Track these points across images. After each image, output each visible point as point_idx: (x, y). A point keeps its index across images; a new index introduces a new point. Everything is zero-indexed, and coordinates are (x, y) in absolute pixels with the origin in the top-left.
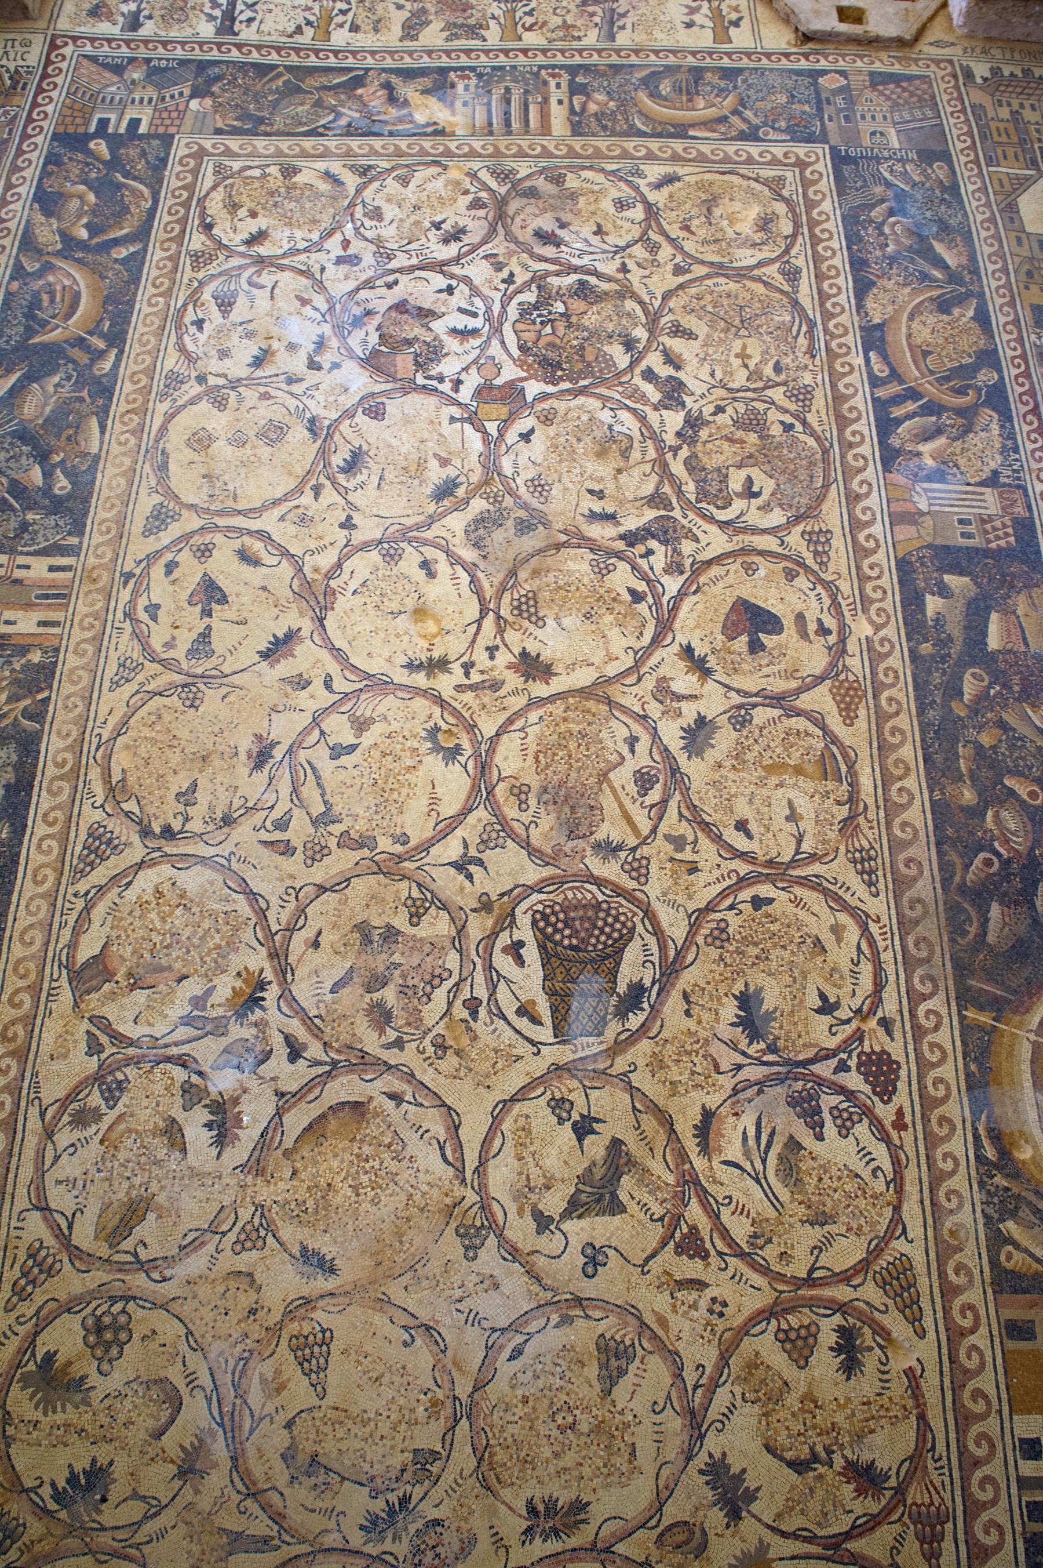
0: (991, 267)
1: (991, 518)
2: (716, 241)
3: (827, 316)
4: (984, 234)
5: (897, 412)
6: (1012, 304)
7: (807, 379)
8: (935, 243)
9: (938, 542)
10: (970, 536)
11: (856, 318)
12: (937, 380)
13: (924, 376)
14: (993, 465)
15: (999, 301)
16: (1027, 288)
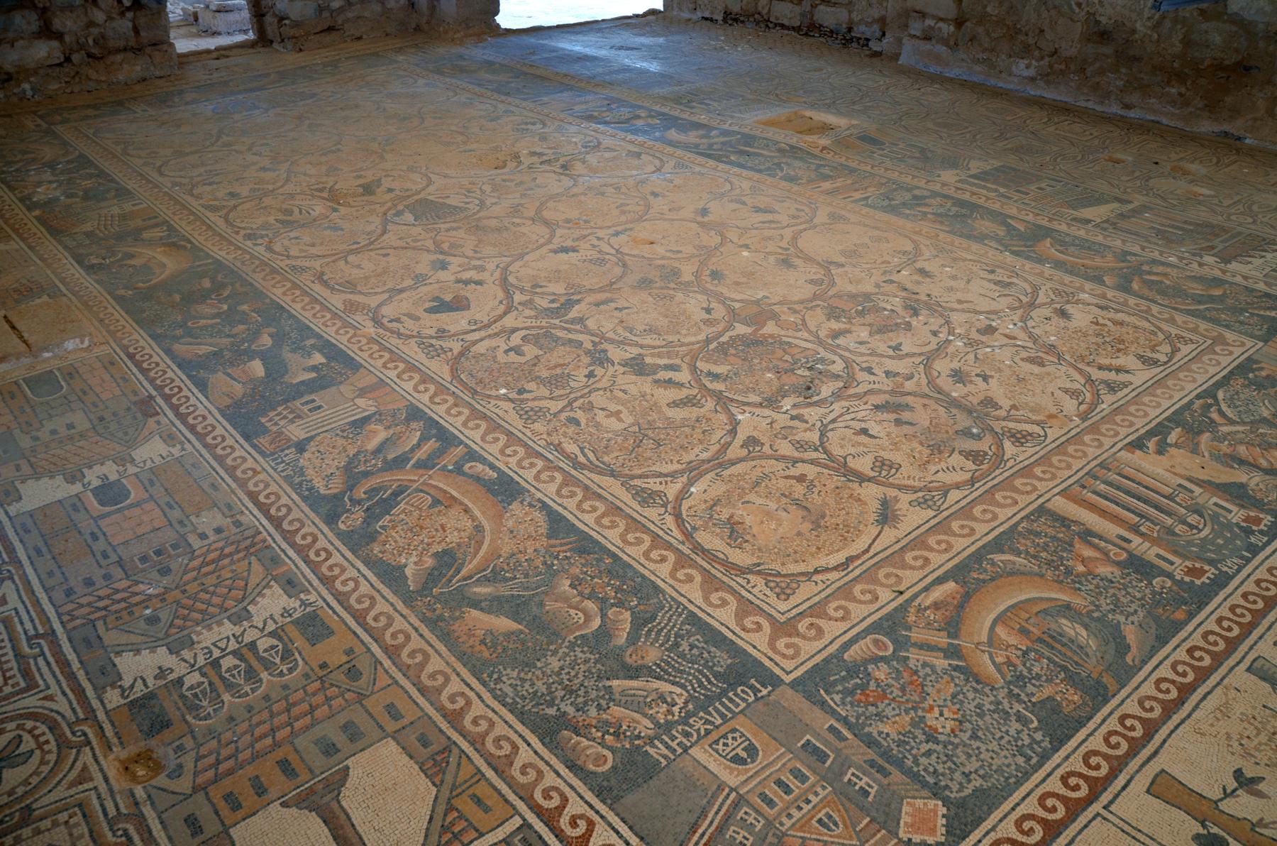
0: (416, 642)
1: (292, 421)
2: (758, 484)
3: (568, 480)
4: (455, 686)
5: (431, 445)
6: (359, 617)
7: (538, 426)
8: (515, 626)
9: (334, 389)
10: (307, 403)
11: (539, 495)
12: (407, 488)
13: (424, 483)
14: (307, 455)
15: (381, 606)
16: (349, 652)
